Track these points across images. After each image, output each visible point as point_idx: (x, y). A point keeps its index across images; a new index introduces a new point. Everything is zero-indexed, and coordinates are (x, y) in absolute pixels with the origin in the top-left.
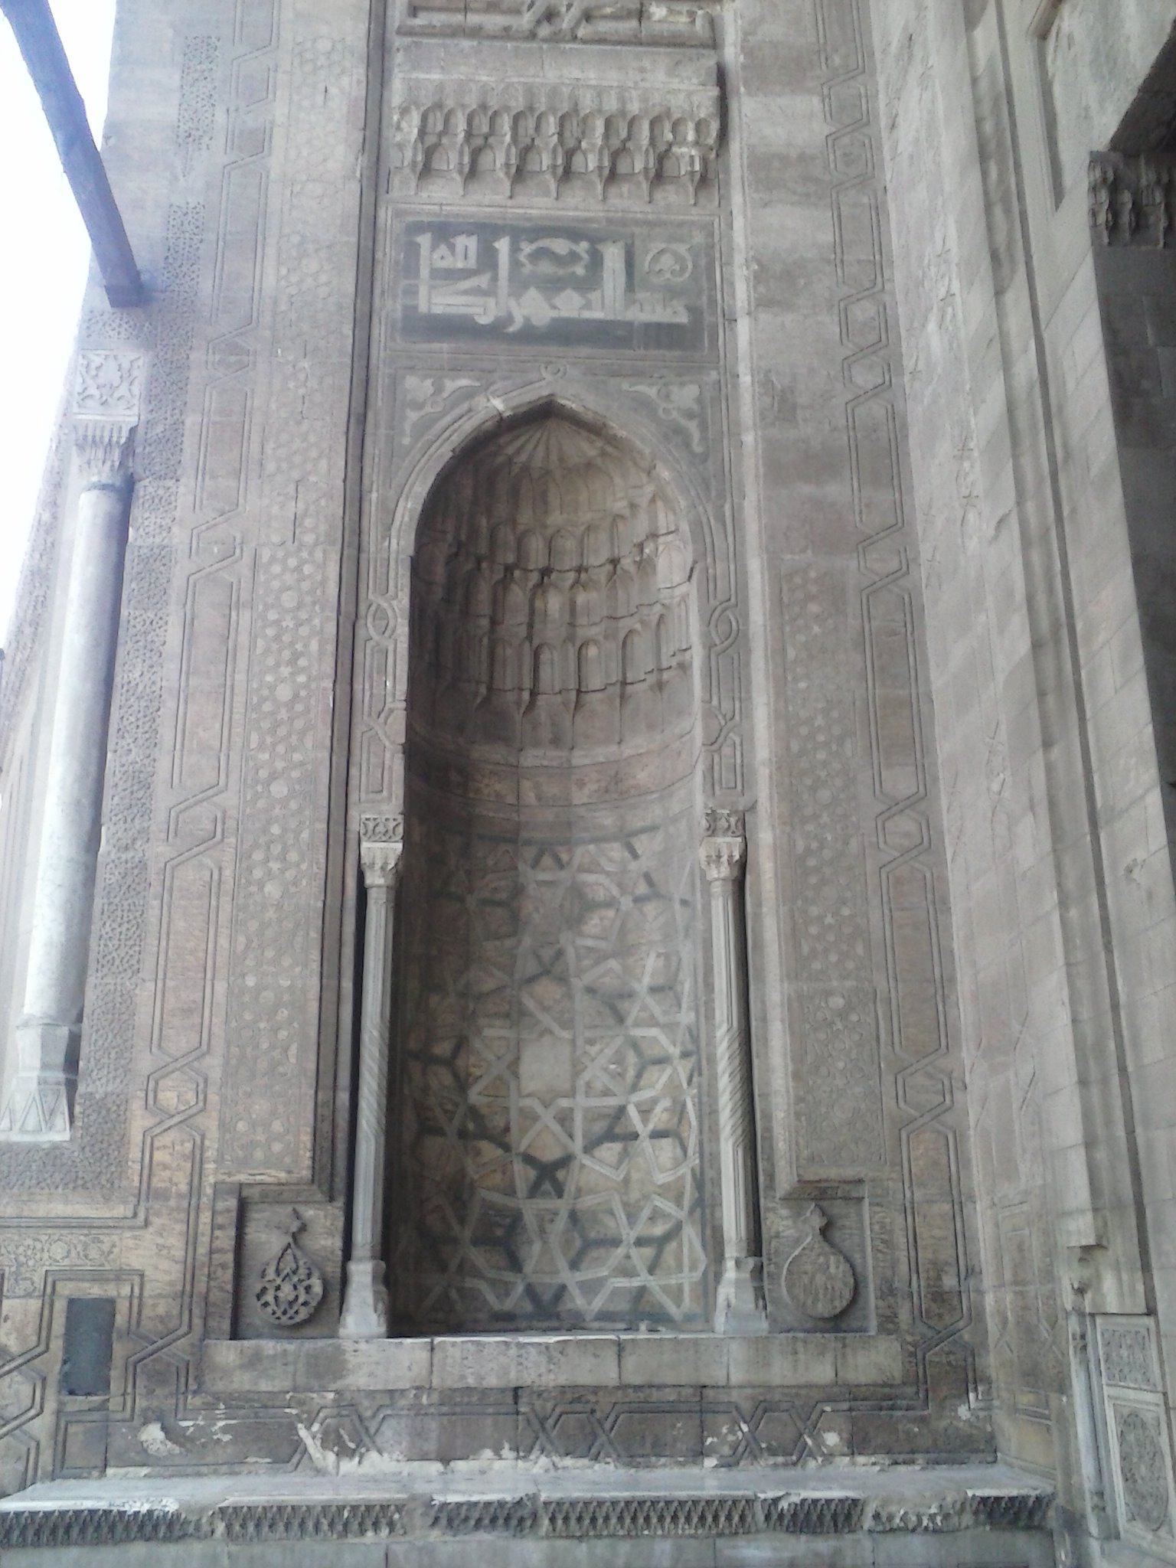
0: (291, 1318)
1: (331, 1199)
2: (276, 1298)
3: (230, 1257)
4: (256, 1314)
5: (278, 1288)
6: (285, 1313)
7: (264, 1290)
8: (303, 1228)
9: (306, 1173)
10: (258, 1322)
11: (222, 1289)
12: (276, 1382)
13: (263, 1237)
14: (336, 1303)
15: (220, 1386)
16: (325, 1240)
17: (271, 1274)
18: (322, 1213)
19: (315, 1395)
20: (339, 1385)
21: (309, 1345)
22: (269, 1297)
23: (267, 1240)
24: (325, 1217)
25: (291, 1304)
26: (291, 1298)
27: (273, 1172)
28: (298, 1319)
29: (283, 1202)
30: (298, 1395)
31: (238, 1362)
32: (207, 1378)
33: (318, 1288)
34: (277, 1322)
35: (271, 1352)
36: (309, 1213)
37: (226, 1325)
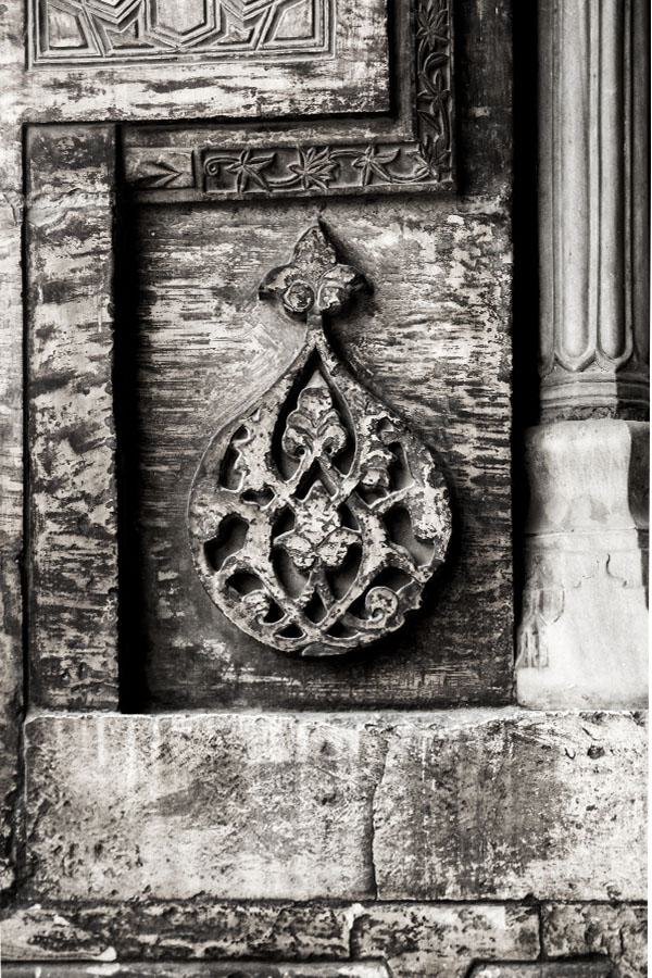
0: (338, 630)
1: (463, 189)
2: (279, 556)
3: (96, 405)
4: (218, 625)
5: (283, 520)
6: (312, 611)
7: (232, 530)
8: (361, 297)
9: (365, 73)
10: (218, 648)
11: (78, 525)
12: (301, 864)
13: (217, 334)
14: (502, 576)
15: (95, 878)
16: (441, 344)
17: (254, 469)
18: (428, 241)
19: (447, 916)
20: (538, 878)
21: (409, 726)
22: (253, 553)
23: (231, 347)
24: (444, 254)
25: (336, 577)
26: (331, 556)
27: (239, 72)
28: (365, 633)
29: (284, 202)
30: (385, 916)
31: (155, 792)
32: (43, 848)
33: (432, 519)
34: (288, 645)
35: (279, 756)
36: (379, 239)
37: (102, 655)
